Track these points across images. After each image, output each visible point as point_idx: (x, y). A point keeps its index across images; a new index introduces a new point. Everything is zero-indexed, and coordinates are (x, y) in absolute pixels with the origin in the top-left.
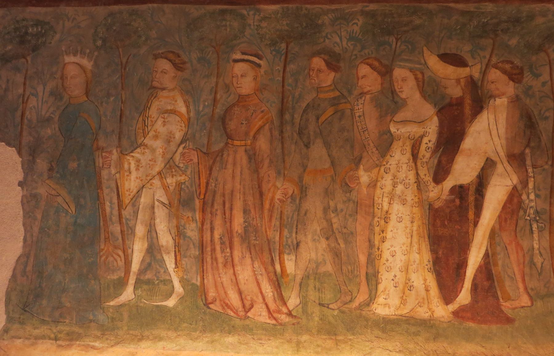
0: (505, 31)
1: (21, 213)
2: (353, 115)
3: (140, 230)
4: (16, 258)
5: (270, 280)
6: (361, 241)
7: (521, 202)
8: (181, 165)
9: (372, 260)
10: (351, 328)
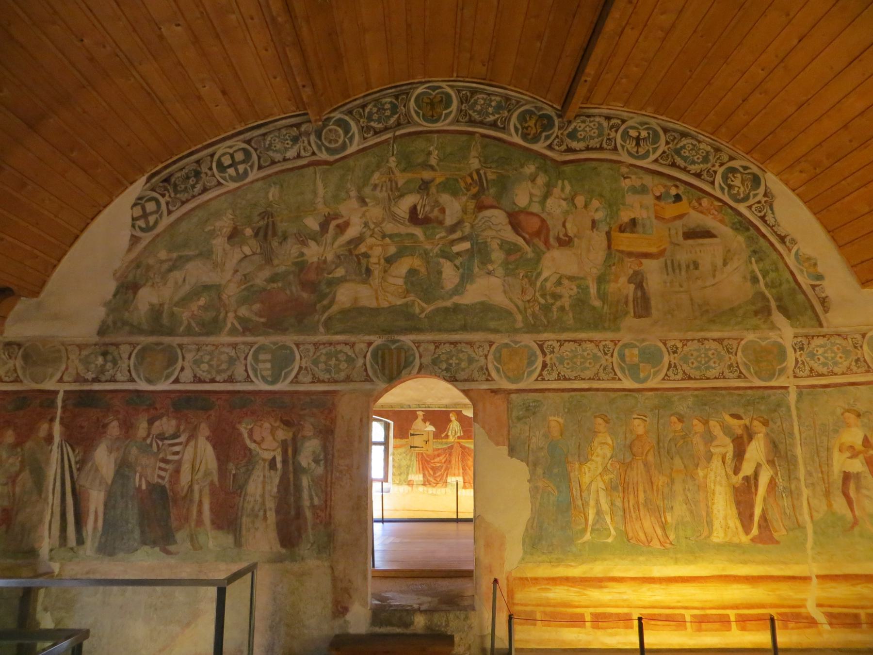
0: (758, 403)
3: (592, 503)
5: (660, 526)
7: (776, 483)
9: (709, 514)
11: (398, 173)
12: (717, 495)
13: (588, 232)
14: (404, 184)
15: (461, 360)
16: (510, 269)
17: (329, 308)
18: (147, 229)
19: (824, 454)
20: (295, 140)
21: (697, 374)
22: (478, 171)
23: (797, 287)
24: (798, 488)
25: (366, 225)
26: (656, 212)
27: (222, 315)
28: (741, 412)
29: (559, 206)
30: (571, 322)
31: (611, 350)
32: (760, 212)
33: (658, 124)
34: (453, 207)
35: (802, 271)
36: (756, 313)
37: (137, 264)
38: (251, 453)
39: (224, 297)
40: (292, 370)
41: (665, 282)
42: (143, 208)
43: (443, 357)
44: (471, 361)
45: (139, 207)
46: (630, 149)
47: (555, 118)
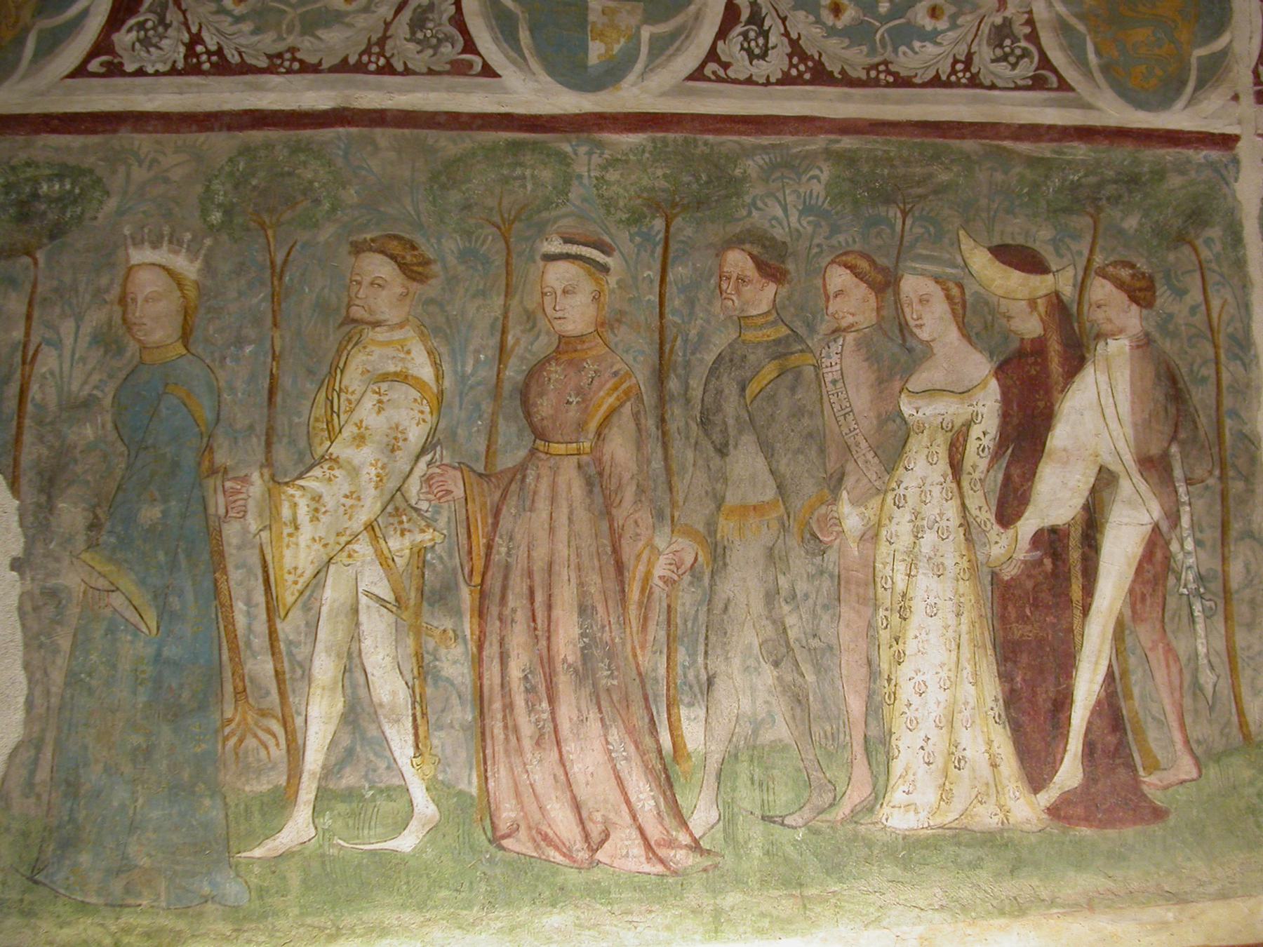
0: (1115, 200)
1: (19, 636)
2: (819, 378)
3: (324, 667)
4: (7, 751)
6: (850, 666)
7: (1168, 557)
8: (424, 506)
9: (875, 707)
10: (834, 868)
12: (918, 616)
21: (856, 58)
28: (1041, 238)
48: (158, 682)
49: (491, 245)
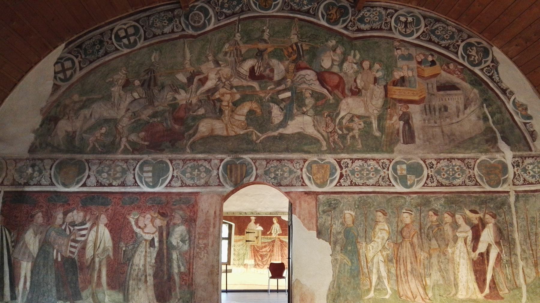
0: (489, 202)
3: (375, 271)
7: (501, 257)
9: (455, 279)
11: (241, 44)
13: (372, 86)
14: (246, 52)
15: (284, 172)
16: (318, 112)
17: (194, 135)
18: (66, 80)
19: (533, 238)
20: (170, 20)
21: (447, 182)
22: (296, 44)
23: (514, 124)
24: (516, 261)
25: (219, 79)
26: (418, 72)
27: (118, 140)
28: (477, 208)
29: (352, 68)
30: (360, 146)
31: (387, 165)
32: (489, 73)
33: (420, 13)
34: (279, 68)
35: (517, 114)
36: (487, 141)
37: (57, 103)
38: (136, 236)
39: (119, 127)
40: (167, 177)
41: (424, 120)
42: (63, 66)
43: (273, 170)
44: (291, 172)
45: (60, 65)
46: (400, 30)
47: (350, 8)
48: (351, 272)
49: (395, 210)
